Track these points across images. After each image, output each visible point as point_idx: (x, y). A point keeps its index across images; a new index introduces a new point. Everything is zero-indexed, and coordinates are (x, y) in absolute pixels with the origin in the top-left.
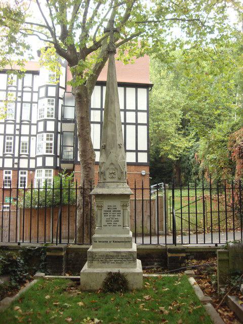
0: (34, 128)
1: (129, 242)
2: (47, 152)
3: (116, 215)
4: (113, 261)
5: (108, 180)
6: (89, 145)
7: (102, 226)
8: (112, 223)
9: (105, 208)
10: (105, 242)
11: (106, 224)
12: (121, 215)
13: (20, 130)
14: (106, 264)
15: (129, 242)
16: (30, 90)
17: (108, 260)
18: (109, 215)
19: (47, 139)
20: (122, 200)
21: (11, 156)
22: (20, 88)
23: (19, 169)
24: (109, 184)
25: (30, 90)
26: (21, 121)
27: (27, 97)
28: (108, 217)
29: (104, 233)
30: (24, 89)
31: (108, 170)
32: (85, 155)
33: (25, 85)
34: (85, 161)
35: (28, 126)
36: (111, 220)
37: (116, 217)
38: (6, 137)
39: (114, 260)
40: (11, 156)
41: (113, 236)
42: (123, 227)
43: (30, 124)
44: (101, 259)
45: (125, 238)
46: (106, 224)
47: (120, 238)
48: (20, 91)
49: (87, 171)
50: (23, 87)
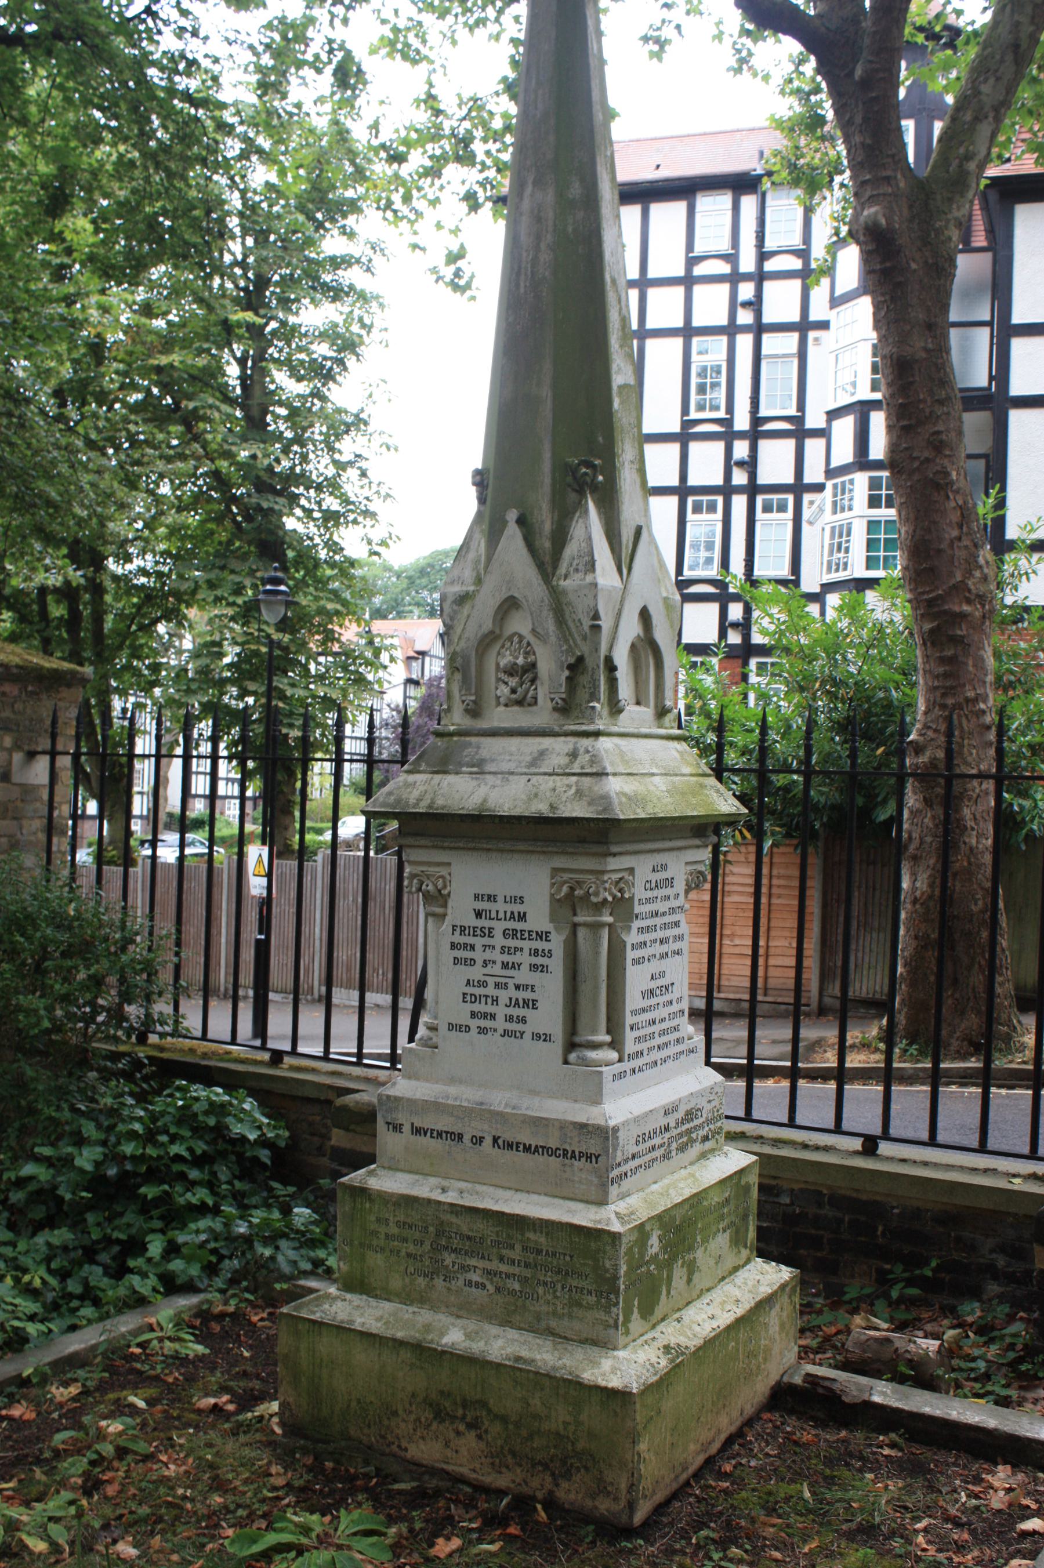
0: (814, 448)
1: (589, 1157)
2: (871, 563)
3: (525, 959)
4: (475, 1277)
5: (500, 717)
6: (955, 517)
7: (443, 1028)
8: (501, 1011)
9: (461, 909)
10: (450, 1135)
11: (462, 1014)
12: (557, 964)
13: (751, 465)
14: (439, 1282)
15: (589, 1157)
16: (796, 264)
17: (449, 1259)
18: (478, 955)
19: (874, 502)
20: (560, 862)
21: (709, 589)
22: (747, 263)
23: (747, 650)
24: (490, 746)
25: (796, 264)
26: (757, 420)
27: (781, 301)
28: (476, 973)
29: (452, 1080)
30: (769, 266)
31: (497, 647)
32: (932, 570)
33: (770, 245)
34: (930, 603)
35: (790, 444)
36: (490, 990)
37: (524, 976)
38: (690, 500)
39: (481, 1264)
40: (709, 589)
41: (499, 1100)
42: (571, 1046)
43: (799, 431)
44: (412, 1248)
45: (563, 1126)
46: (462, 1014)
47: (539, 1123)
48: (747, 277)
49: (942, 660)
50: (763, 256)
